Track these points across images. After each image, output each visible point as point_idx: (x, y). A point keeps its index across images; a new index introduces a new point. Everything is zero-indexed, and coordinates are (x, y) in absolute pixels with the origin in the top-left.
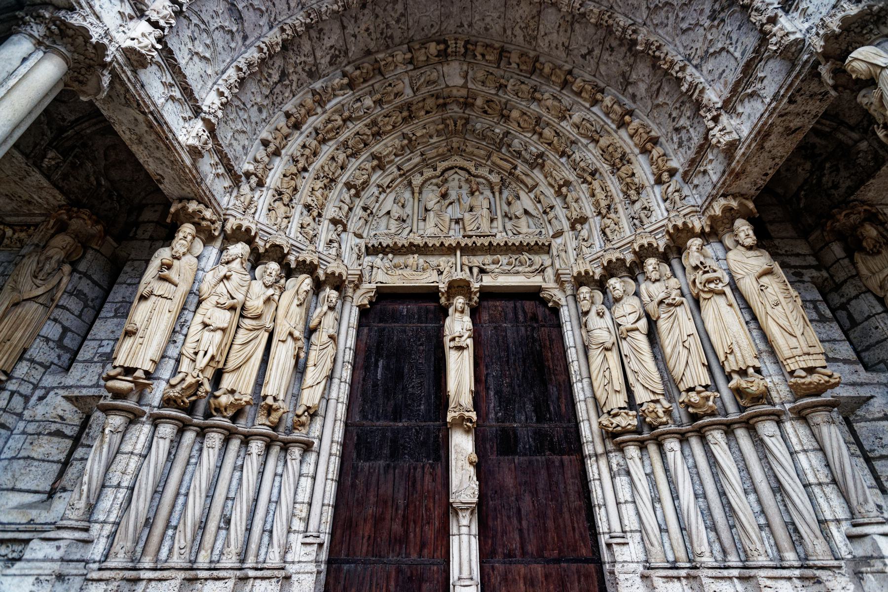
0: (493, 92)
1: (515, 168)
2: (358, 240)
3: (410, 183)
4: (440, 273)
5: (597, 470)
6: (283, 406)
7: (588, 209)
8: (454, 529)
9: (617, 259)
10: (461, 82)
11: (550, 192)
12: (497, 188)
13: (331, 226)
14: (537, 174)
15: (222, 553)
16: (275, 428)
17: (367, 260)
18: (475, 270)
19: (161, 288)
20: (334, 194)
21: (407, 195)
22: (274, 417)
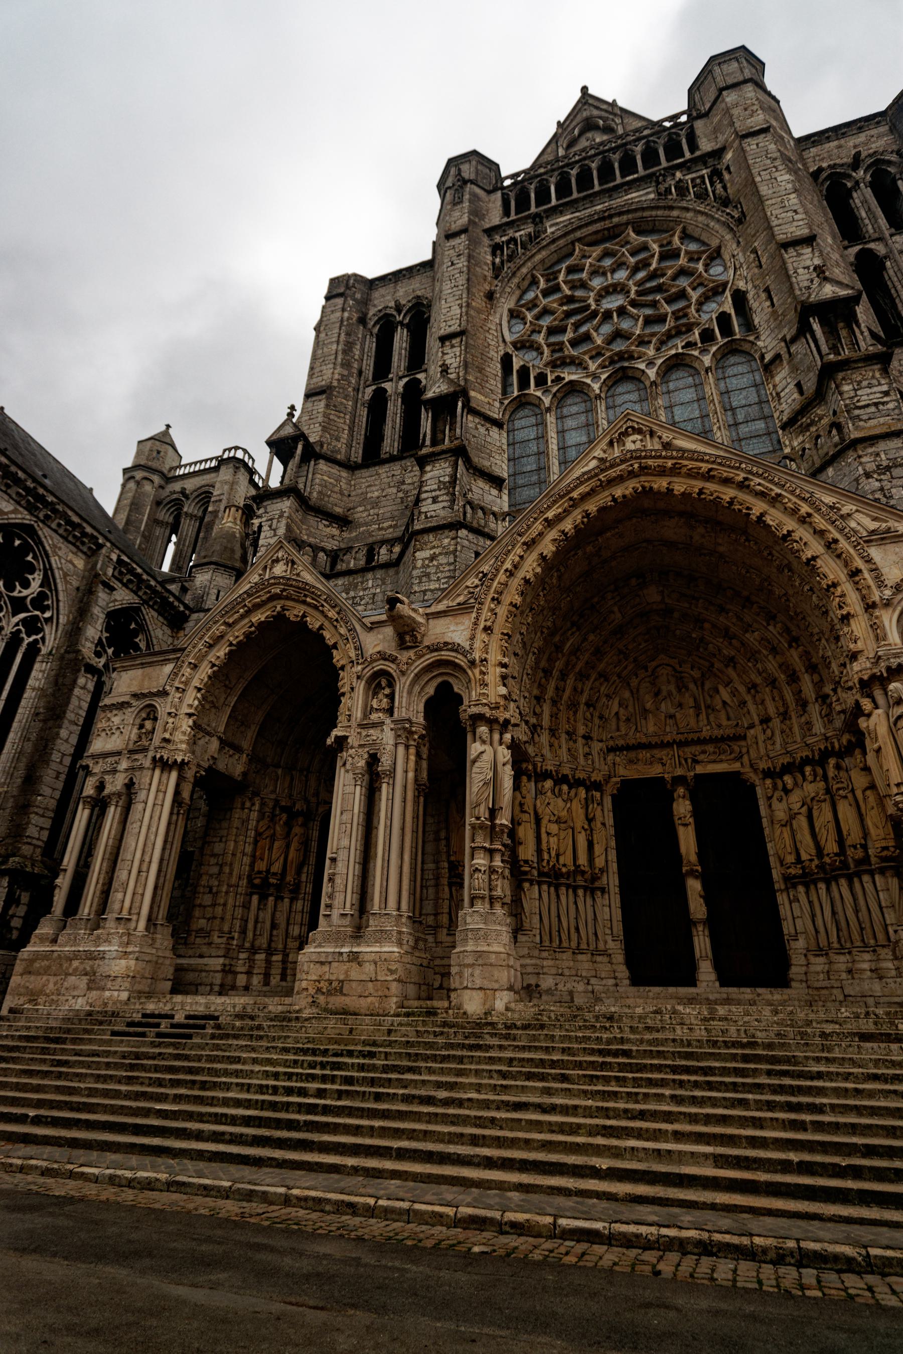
0: (686, 605)
1: (712, 665)
2: (600, 744)
3: (628, 684)
4: (664, 765)
5: (782, 899)
6: (587, 869)
7: (772, 711)
8: (695, 933)
9: (788, 763)
10: (658, 598)
11: (742, 689)
12: (699, 683)
13: (584, 741)
14: (730, 671)
15: (579, 943)
16: (586, 881)
17: (610, 757)
18: (689, 761)
19: (525, 817)
20: (580, 715)
21: (627, 694)
22: (586, 876)
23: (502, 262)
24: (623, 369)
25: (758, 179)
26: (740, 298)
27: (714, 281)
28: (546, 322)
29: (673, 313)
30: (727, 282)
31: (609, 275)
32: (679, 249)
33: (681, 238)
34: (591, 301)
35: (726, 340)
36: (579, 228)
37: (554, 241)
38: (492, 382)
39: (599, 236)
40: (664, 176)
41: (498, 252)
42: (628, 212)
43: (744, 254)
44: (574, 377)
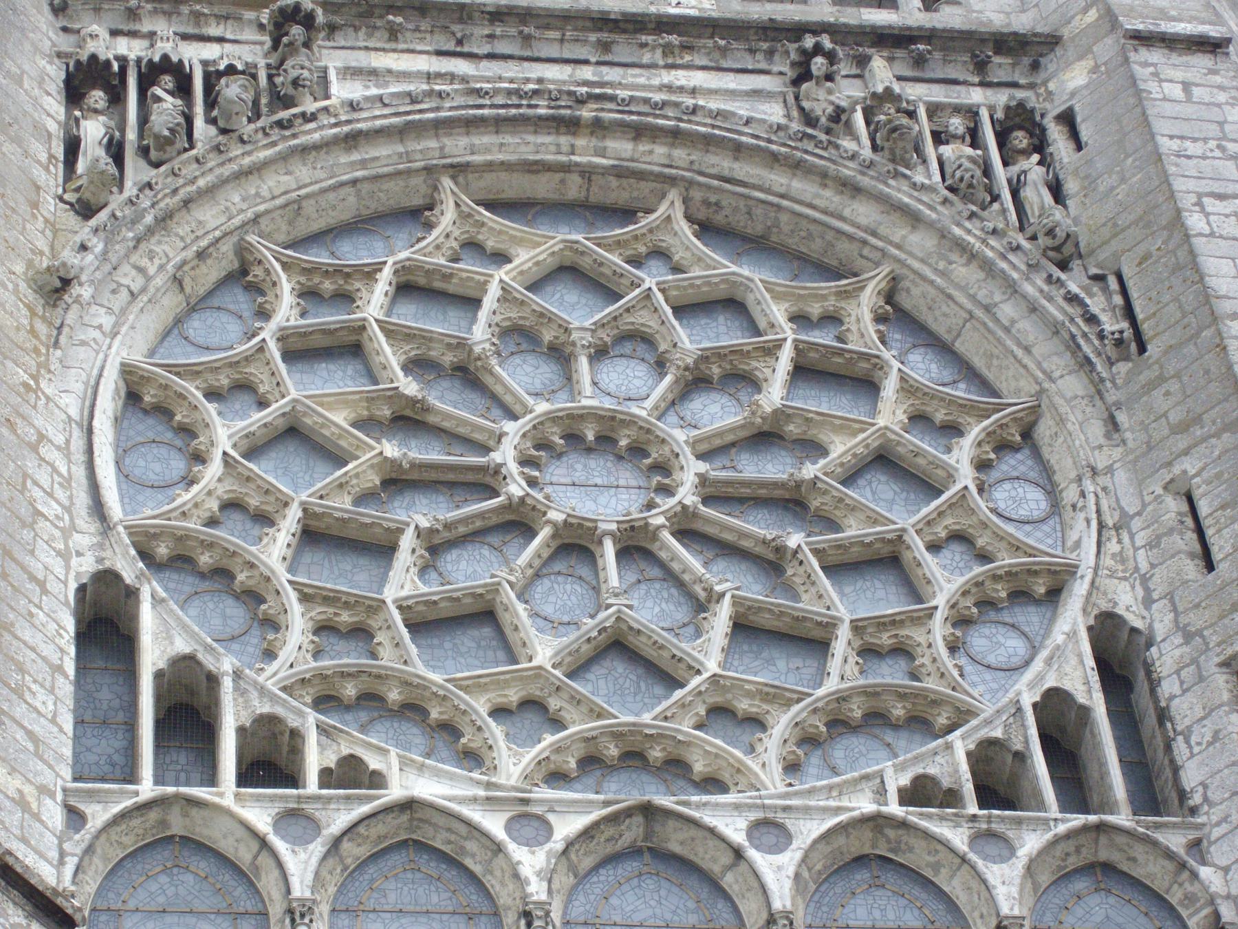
23: (116, 150)
24: (648, 810)
25: (1195, 222)
26: (1119, 658)
27: (1016, 547)
28: (300, 487)
29: (858, 627)
30: (1071, 571)
31: (583, 363)
32: (879, 365)
33: (880, 319)
34: (506, 455)
35: (1078, 820)
36: (471, 124)
37: (352, 140)
38: (42, 700)
39: (543, 187)
40: (831, 57)
41: (97, 97)
42: (675, 136)
43: (1140, 484)
44: (428, 788)
